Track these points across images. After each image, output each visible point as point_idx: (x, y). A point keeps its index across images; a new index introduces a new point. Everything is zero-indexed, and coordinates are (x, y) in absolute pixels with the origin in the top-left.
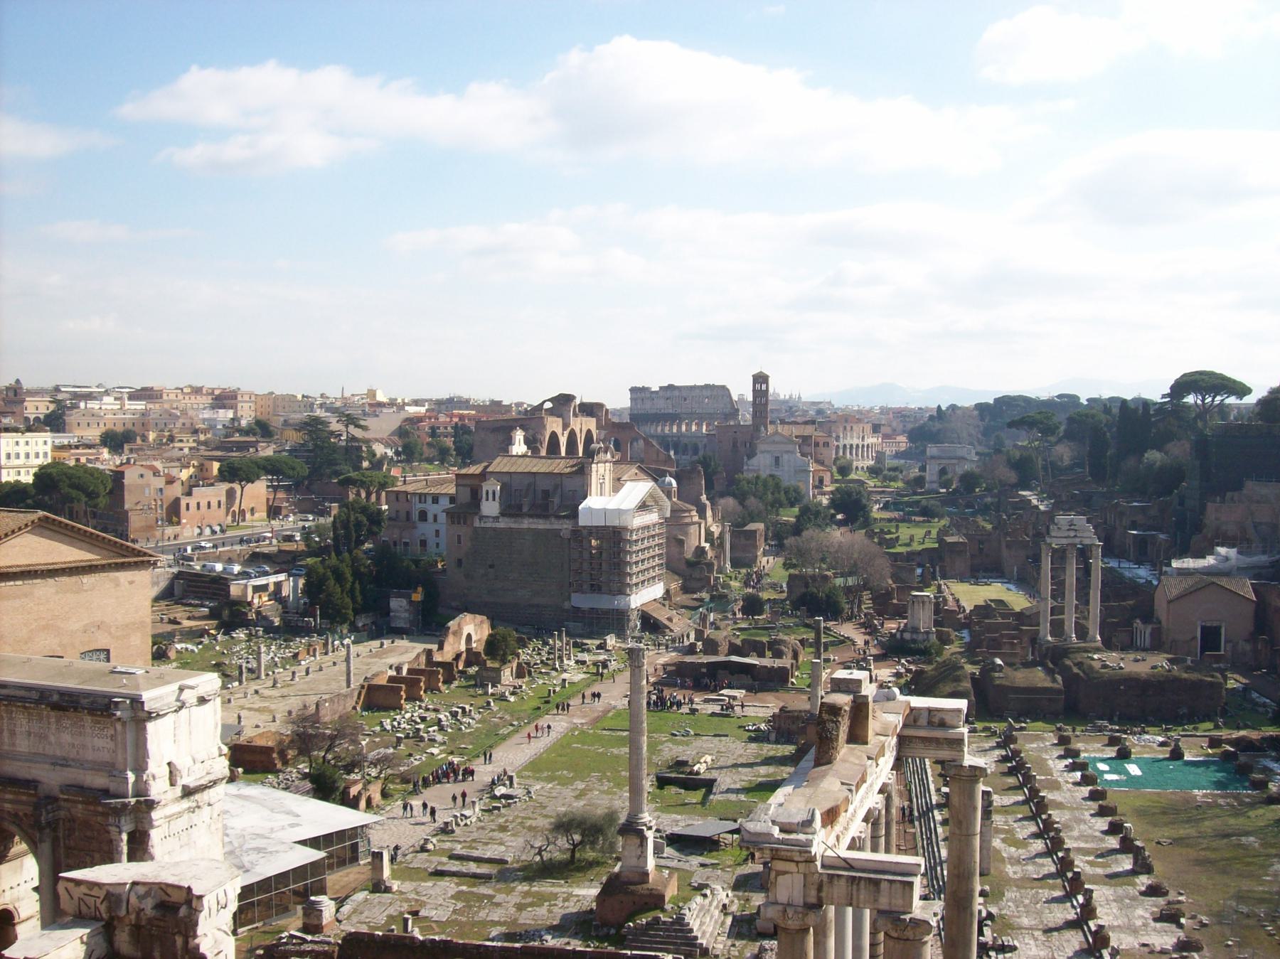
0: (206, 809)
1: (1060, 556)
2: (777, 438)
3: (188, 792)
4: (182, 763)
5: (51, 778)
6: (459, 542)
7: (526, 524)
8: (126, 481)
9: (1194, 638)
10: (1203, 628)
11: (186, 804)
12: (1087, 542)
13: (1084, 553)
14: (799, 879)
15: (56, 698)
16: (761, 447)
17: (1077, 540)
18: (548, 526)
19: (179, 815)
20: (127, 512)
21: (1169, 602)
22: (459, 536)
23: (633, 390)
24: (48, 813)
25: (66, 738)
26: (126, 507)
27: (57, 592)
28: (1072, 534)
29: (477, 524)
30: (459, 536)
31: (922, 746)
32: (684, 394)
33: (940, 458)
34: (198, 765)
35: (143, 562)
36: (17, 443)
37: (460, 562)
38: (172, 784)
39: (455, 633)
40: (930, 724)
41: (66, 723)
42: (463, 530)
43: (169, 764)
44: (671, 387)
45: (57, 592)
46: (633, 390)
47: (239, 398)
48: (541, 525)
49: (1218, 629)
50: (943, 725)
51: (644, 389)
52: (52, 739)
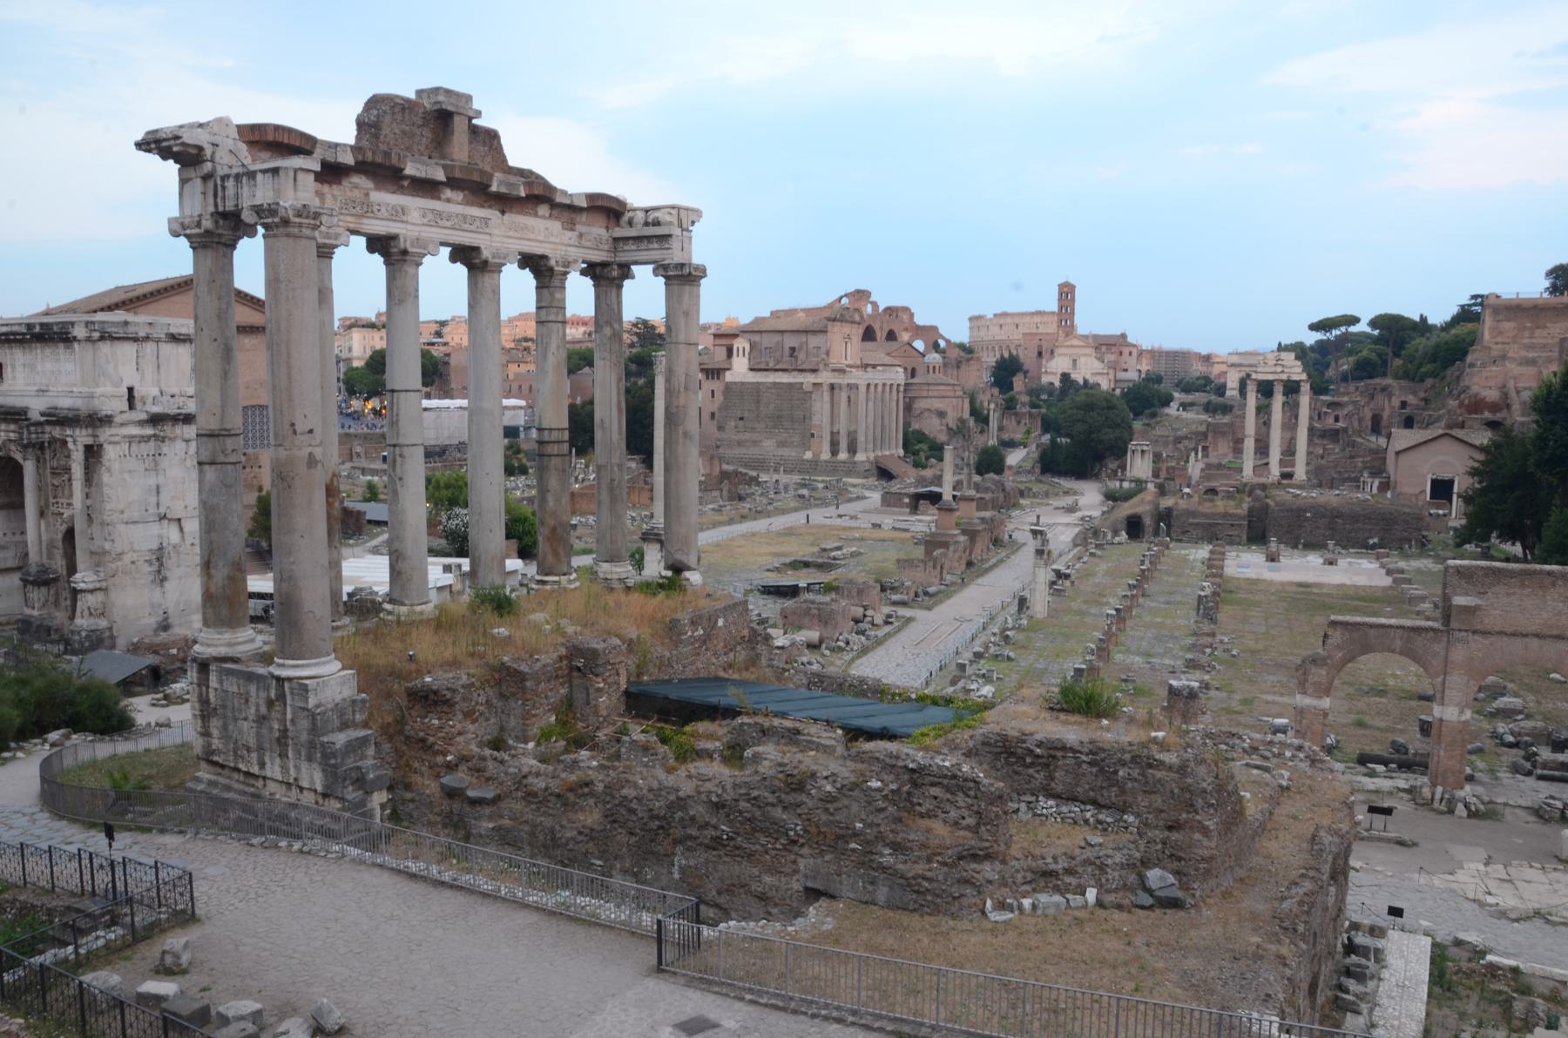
0: (179, 446)
1: (1266, 389)
2: (1076, 342)
3: (155, 420)
4: (147, 389)
5: (37, 407)
7: (772, 378)
9: (1424, 491)
10: (1434, 482)
11: (149, 431)
12: (1295, 377)
13: (1292, 388)
15: (37, 329)
16: (1058, 351)
17: (1284, 377)
18: (792, 380)
19: (145, 439)
21: (1398, 453)
23: (971, 319)
25: (48, 366)
28: (1279, 369)
32: (1016, 320)
33: (1240, 365)
34: (166, 398)
38: (131, 406)
40: (646, 224)
41: (48, 351)
42: (716, 385)
43: (130, 390)
44: (1005, 315)
46: (971, 319)
48: (784, 378)
49: (1451, 482)
50: (657, 223)
51: (979, 318)
52: (39, 368)
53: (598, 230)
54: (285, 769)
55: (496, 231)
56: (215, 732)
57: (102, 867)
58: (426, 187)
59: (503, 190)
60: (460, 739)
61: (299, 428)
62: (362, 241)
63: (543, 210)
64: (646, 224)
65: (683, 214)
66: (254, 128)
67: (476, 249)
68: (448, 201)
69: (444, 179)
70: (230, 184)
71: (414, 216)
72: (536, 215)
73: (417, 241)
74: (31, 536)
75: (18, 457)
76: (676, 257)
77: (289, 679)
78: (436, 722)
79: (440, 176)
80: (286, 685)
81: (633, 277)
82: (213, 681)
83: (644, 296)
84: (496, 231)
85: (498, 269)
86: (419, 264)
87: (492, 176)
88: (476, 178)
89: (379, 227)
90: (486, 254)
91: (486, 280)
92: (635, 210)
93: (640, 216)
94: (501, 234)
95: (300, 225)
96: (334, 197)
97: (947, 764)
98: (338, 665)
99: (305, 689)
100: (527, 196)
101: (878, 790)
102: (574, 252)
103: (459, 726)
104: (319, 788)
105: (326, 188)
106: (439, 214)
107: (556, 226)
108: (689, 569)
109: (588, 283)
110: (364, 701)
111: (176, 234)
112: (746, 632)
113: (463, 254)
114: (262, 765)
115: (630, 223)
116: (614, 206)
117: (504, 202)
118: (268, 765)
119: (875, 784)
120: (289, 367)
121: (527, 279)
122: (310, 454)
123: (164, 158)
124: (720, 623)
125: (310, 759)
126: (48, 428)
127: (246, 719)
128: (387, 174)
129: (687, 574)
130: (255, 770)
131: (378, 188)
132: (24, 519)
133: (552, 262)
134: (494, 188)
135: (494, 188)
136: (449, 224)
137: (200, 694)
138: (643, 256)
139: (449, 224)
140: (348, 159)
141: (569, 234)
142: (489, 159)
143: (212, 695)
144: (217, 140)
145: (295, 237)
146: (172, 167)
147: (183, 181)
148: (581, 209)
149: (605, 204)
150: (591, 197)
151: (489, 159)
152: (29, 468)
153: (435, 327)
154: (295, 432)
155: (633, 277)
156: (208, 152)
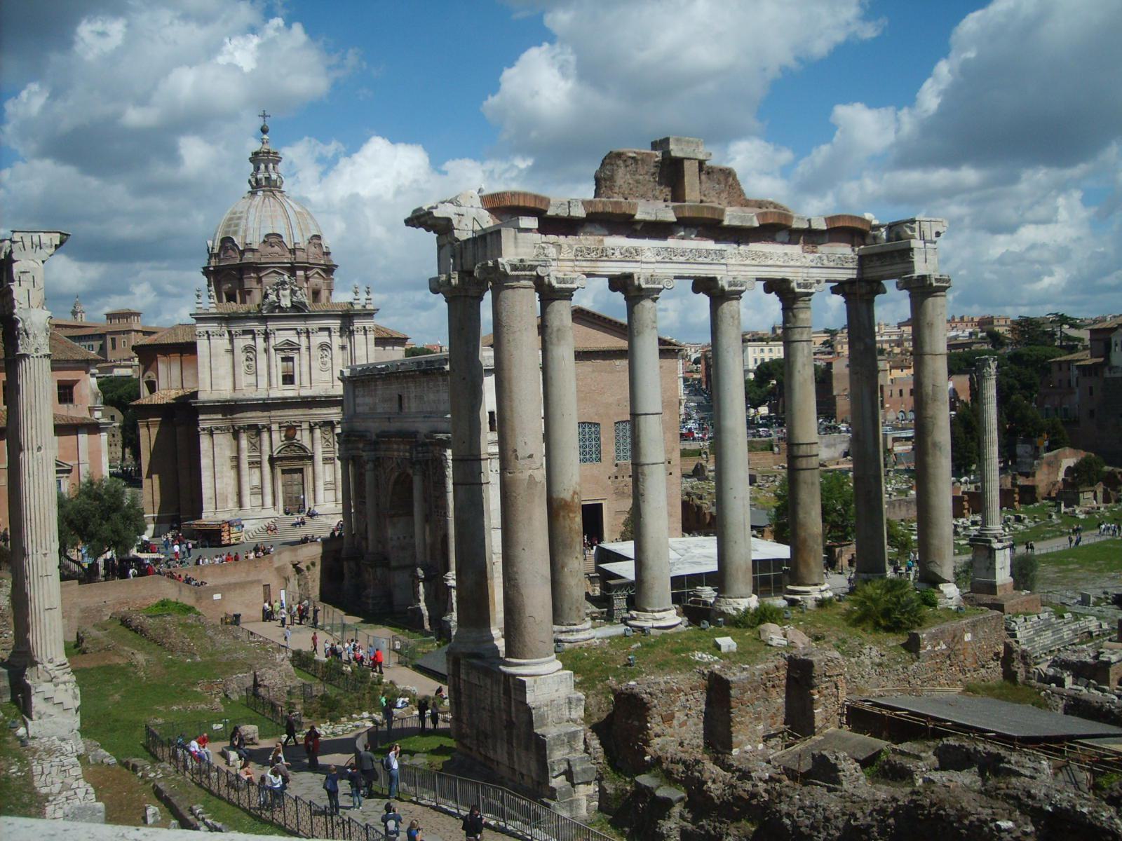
5: (423, 427)
6: (1091, 394)
8: (834, 371)
14: (447, 249)
20: (834, 397)
22: (1091, 388)
24: (418, 453)
25: (432, 396)
26: (835, 393)
27: (593, 371)
29: (1107, 374)
30: (1091, 388)
31: (878, 263)
35: (668, 350)
36: (762, 350)
37: (1092, 413)
39: (1049, 464)
41: (431, 384)
45: (593, 371)
47: (995, 323)
50: (899, 238)
53: (845, 250)
54: (510, 755)
55: (732, 261)
56: (465, 719)
57: (338, 824)
58: (658, 230)
59: (736, 223)
60: (657, 740)
61: (521, 453)
62: (606, 280)
63: (782, 235)
64: (889, 240)
65: (926, 226)
66: (494, 197)
67: (714, 280)
68: (683, 238)
69: (675, 220)
70: (470, 246)
71: (649, 256)
72: (774, 240)
73: (652, 278)
74: (418, 540)
75: (410, 472)
76: (920, 269)
77: (514, 676)
78: (636, 723)
79: (670, 217)
80: (511, 680)
81: (885, 292)
82: (463, 676)
83: (891, 310)
84: (732, 261)
85: (737, 295)
86: (655, 300)
87: (722, 211)
88: (707, 215)
89: (617, 269)
90: (724, 283)
91: (728, 308)
92: (877, 228)
93: (883, 233)
94: (736, 264)
95: (518, 278)
96: (570, 246)
97: (1085, 810)
98: (559, 664)
99: (522, 685)
100: (761, 226)
101: (1009, 831)
102: (817, 274)
103: (657, 729)
104: (534, 775)
105: (562, 239)
106: (673, 251)
107: (795, 250)
108: (944, 581)
109: (838, 301)
110: (579, 700)
111: (435, 291)
112: (1001, 648)
113: (704, 285)
114: (495, 751)
115: (875, 237)
116: (860, 226)
117: (740, 235)
118: (499, 751)
119: (1005, 824)
120: (511, 400)
121: (774, 303)
122: (530, 476)
123: (428, 230)
124: (968, 637)
125: (527, 749)
126: (431, 448)
127: (484, 709)
128: (624, 224)
129: (942, 586)
130: (491, 754)
131: (611, 234)
132: (413, 526)
133: (794, 285)
134: (726, 223)
135: (726, 223)
136: (682, 259)
137: (454, 685)
138: (888, 270)
139: (682, 259)
140: (579, 212)
141: (811, 256)
142: (724, 195)
143: (462, 686)
144: (462, 210)
145: (513, 288)
146: (432, 236)
147: (440, 247)
148: (821, 232)
149: (847, 224)
150: (829, 220)
151: (724, 195)
152: (417, 481)
153: (825, 337)
154: (517, 457)
155: (885, 292)
156: (455, 223)
